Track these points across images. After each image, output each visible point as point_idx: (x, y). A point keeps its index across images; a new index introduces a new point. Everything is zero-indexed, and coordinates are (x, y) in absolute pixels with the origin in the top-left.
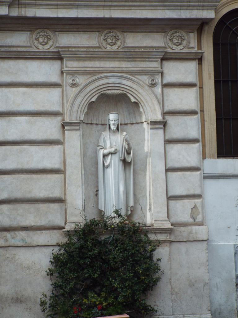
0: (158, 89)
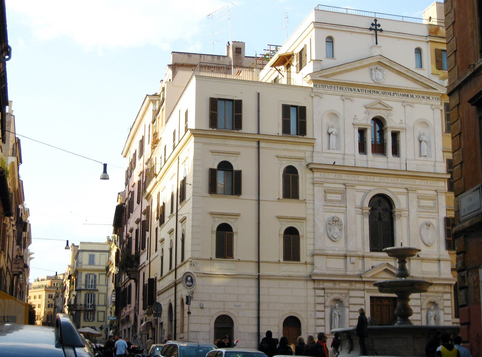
0: (442, 301)
